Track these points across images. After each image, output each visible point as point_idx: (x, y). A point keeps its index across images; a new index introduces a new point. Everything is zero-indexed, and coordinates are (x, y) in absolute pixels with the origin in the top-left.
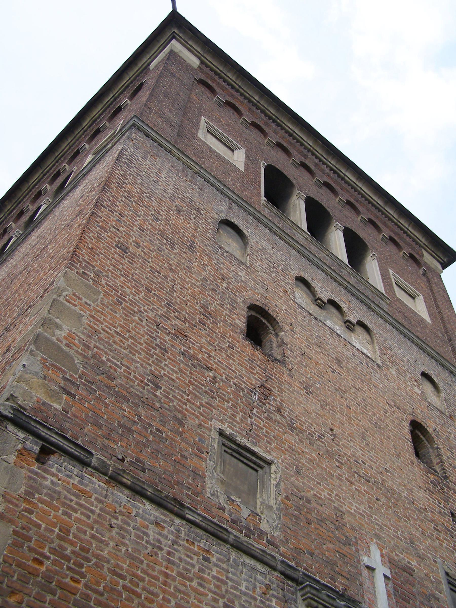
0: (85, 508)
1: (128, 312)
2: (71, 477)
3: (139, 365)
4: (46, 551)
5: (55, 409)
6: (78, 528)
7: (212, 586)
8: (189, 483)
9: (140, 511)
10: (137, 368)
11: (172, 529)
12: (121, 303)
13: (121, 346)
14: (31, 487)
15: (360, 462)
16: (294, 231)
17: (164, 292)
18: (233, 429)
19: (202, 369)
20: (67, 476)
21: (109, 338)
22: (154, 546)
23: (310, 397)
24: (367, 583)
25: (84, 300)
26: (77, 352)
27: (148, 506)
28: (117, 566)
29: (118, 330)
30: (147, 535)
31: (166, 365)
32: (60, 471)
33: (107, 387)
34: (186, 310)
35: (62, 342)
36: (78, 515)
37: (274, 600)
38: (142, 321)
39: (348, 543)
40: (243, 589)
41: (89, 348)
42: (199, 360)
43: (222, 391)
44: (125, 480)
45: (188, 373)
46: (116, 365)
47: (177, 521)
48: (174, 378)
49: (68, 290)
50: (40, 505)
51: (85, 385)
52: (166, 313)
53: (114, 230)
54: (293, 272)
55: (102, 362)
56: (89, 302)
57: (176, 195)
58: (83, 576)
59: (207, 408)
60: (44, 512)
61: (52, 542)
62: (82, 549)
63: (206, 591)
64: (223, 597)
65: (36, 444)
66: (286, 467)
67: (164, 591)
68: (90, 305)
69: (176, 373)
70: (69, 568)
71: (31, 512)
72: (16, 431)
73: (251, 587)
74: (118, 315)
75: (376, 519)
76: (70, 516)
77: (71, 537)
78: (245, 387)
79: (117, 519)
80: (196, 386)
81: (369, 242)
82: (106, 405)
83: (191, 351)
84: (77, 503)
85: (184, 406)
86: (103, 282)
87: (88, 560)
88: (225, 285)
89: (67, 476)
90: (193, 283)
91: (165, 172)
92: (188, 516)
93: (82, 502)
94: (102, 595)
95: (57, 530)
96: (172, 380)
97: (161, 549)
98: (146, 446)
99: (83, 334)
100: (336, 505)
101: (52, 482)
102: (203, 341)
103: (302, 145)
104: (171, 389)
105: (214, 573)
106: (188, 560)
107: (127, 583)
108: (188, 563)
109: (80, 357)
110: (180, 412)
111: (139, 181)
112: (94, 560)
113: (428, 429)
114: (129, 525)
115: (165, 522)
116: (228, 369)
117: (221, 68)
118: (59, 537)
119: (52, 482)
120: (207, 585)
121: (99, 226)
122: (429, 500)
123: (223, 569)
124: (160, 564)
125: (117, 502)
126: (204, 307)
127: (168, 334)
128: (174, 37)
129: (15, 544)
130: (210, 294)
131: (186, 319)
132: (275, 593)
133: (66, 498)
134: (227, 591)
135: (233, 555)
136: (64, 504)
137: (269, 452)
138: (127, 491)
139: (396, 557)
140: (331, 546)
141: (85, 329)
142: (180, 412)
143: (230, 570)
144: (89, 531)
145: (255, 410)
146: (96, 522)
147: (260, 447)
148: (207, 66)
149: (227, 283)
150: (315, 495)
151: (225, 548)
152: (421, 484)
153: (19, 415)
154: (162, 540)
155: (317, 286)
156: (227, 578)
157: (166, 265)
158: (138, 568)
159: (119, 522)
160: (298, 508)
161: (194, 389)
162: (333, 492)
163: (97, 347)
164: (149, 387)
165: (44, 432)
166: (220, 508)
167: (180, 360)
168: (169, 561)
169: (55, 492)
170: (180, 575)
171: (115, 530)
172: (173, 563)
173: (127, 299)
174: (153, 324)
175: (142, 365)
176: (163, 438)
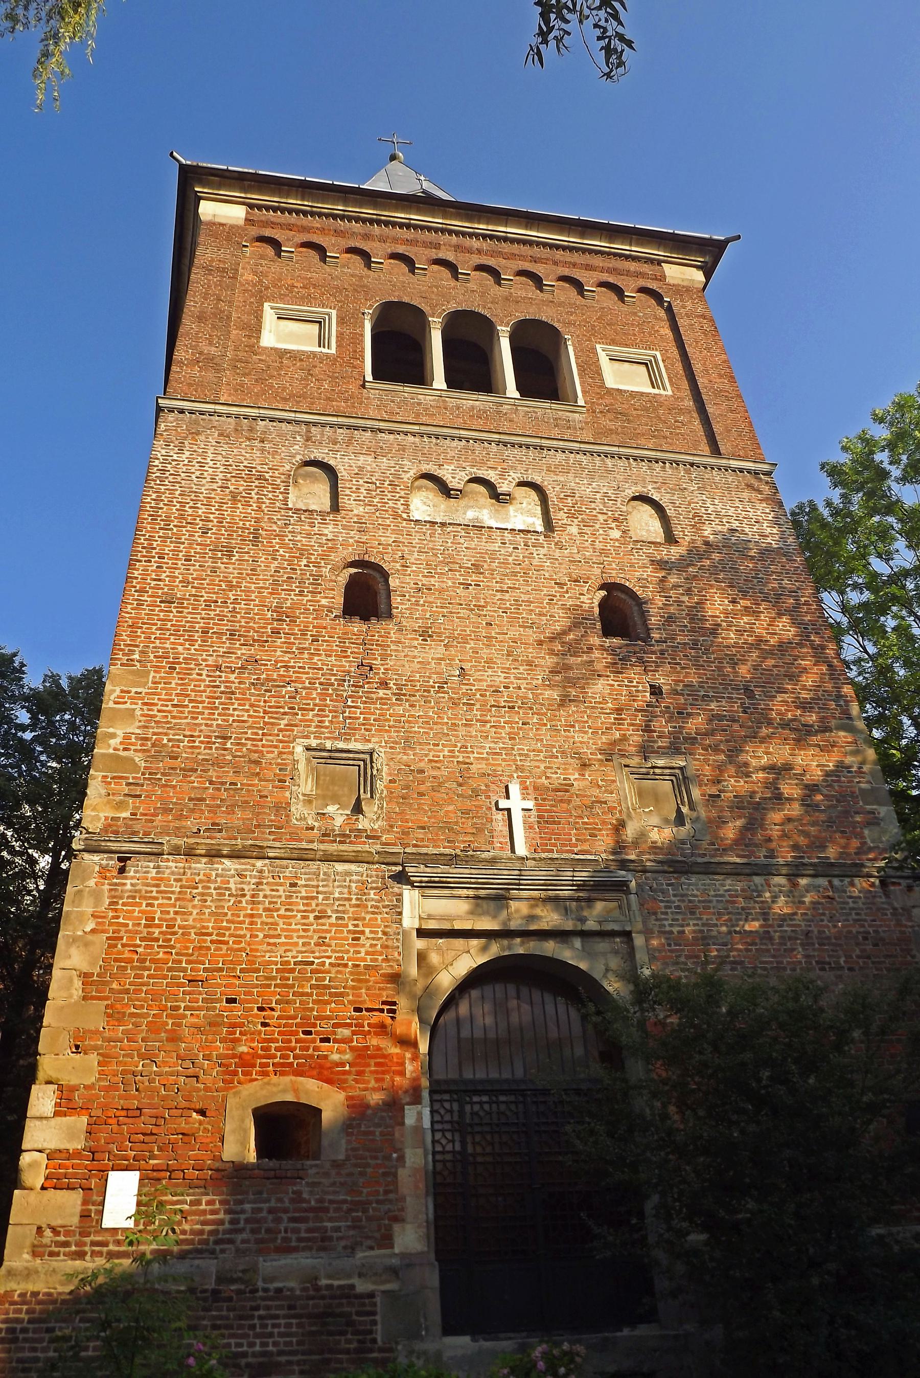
0: (166, 892)
1: (185, 674)
2: (147, 872)
3: (203, 727)
4: (138, 942)
5: (124, 818)
6: (161, 912)
7: (302, 908)
8: (272, 821)
9: (220, 871)
10: (201, 731)
11: (254, 873)
12: (175, 668)
13: (180, 718)
14: (114, 897)
15: (502, 689)
16: (420, 397)
17: (225, 622)
18: (320, 738)
19: (278, 689)
20: (145, 872)
21: (166, 717)
22: (237, 896)
23: (428, 643)
24: (500, 825)
25: (134, 690)
26: (135, 751)
27: (226, 862)
28: (204, 927)
29: (175, 702)
30: (229, 889)
31: (234, 710)
32: (136, 872)
33: (172, 768)
34: (253, 628)
35: (118, 750)
36: (160, 901)
37: (372, 892)
38: (201, 675)
39: (476, 793)
40: (337, 895)
41: (147, 739)
42: (275, 680)
43: (304, 702)
44: (198, 852)
45: (262, 704)
46: (179, 740)
47: (259, 864)
48: (245, 718)
49: (115, 691)
50: (125, 908)
51: (149, 779)
52: (230, 648)
53: (155, 582)
54: (408, 475)
55: (164, 745)
56: (139, 690)
57: (229, 475)
58: (173, 947)
59: (287, 730)
60: (128, 911)
61: (141, 932)
62: (168, 927)
63: (295, 913)
64: (313, 911)
65: (111, 859)
66: (391, 748)
67: (251, 930)
68: (140, 693)
69: (248, 711)
70: (159, 947)
71: (118, 917)
72: (91, 857)
73: (346, 890)
74: (173, 685)
75: (519, 749)
76: (152, 905)
77: (157, 922)
78: (336, 680)
79: (197, 888)
80: (271, 713)
81: (559, 321)
82: (174, 787)
83: (264, 676)
84: (158, 892)
85: (260, 743)
86: (152, 656)
87: (174, 933)
88: (304, 562)
89: (145, 872)
90: (262, 588)
91: (211, 450)
92: (270, 855)
93: (163, 888)
94: (192, 955)
95: (143, 922)
96: (244, 721)
97: (244, 895)
98: (219, 806)
99: (139, 727)
100: (461, 759)
101: (132, 885)
102: (279, 653)
104: (242, 733)
105: (304, 894)
106: (274, 893)
107: (214, 937)
108: (273, 897)
109: (140, 754)
110: (255, 752)
111: (178, 493)
112: (181, 931)
113: (627, 584)
114: (209, 888)
115: (246, 870)
116: (311, 671)
118: (146, 926)
119: (132, 885)
120: (295, 908)
121: (136, 591)
122: (613, 685)
123: (313, 886)
124: (246, 909)
125: (195, 874)
126: (278, 610)
127: (233, 672)
128: (201, 198)
129: (110, 946)
130: (285, 587)
131: (254, 641)
132: (374, 885)
133: (147, 892)
134: (317, 905)
135: (324, 867)
136: (145, 898)
137: (369, 741)
138: (204, 860)
139: (546, 782)
140: (451, 808)
141: (140, 721)
142: (255, 752)
143: (321, 884)
144: (172, 910)
145: (350, 700)
146: (177, 899)
147: (356, 740)
148: (260, 207)
149: (308, 558)
150: (430, 761)
151: (314, 866)
153: (90, 842)
154: (245, 886)
155: (446, 473)
156: (318, 893)
157: (224, 587)
158: (222, 921)
159: (200, 890)
160: (407, 787)
161: (270, 718)
162: (456, 746)
163: (154, 734)
164: (217, 745)
165: (114, 846)
166: (308, 829)
167: (252, 695)
168: (253, 903)
169: (136, 891)
170: (265, 910)
171: (198, 898)
172: (259, 903)
173: (181, 660)
174: (214, 671)
175: (206, 725)
176: (238, 789)
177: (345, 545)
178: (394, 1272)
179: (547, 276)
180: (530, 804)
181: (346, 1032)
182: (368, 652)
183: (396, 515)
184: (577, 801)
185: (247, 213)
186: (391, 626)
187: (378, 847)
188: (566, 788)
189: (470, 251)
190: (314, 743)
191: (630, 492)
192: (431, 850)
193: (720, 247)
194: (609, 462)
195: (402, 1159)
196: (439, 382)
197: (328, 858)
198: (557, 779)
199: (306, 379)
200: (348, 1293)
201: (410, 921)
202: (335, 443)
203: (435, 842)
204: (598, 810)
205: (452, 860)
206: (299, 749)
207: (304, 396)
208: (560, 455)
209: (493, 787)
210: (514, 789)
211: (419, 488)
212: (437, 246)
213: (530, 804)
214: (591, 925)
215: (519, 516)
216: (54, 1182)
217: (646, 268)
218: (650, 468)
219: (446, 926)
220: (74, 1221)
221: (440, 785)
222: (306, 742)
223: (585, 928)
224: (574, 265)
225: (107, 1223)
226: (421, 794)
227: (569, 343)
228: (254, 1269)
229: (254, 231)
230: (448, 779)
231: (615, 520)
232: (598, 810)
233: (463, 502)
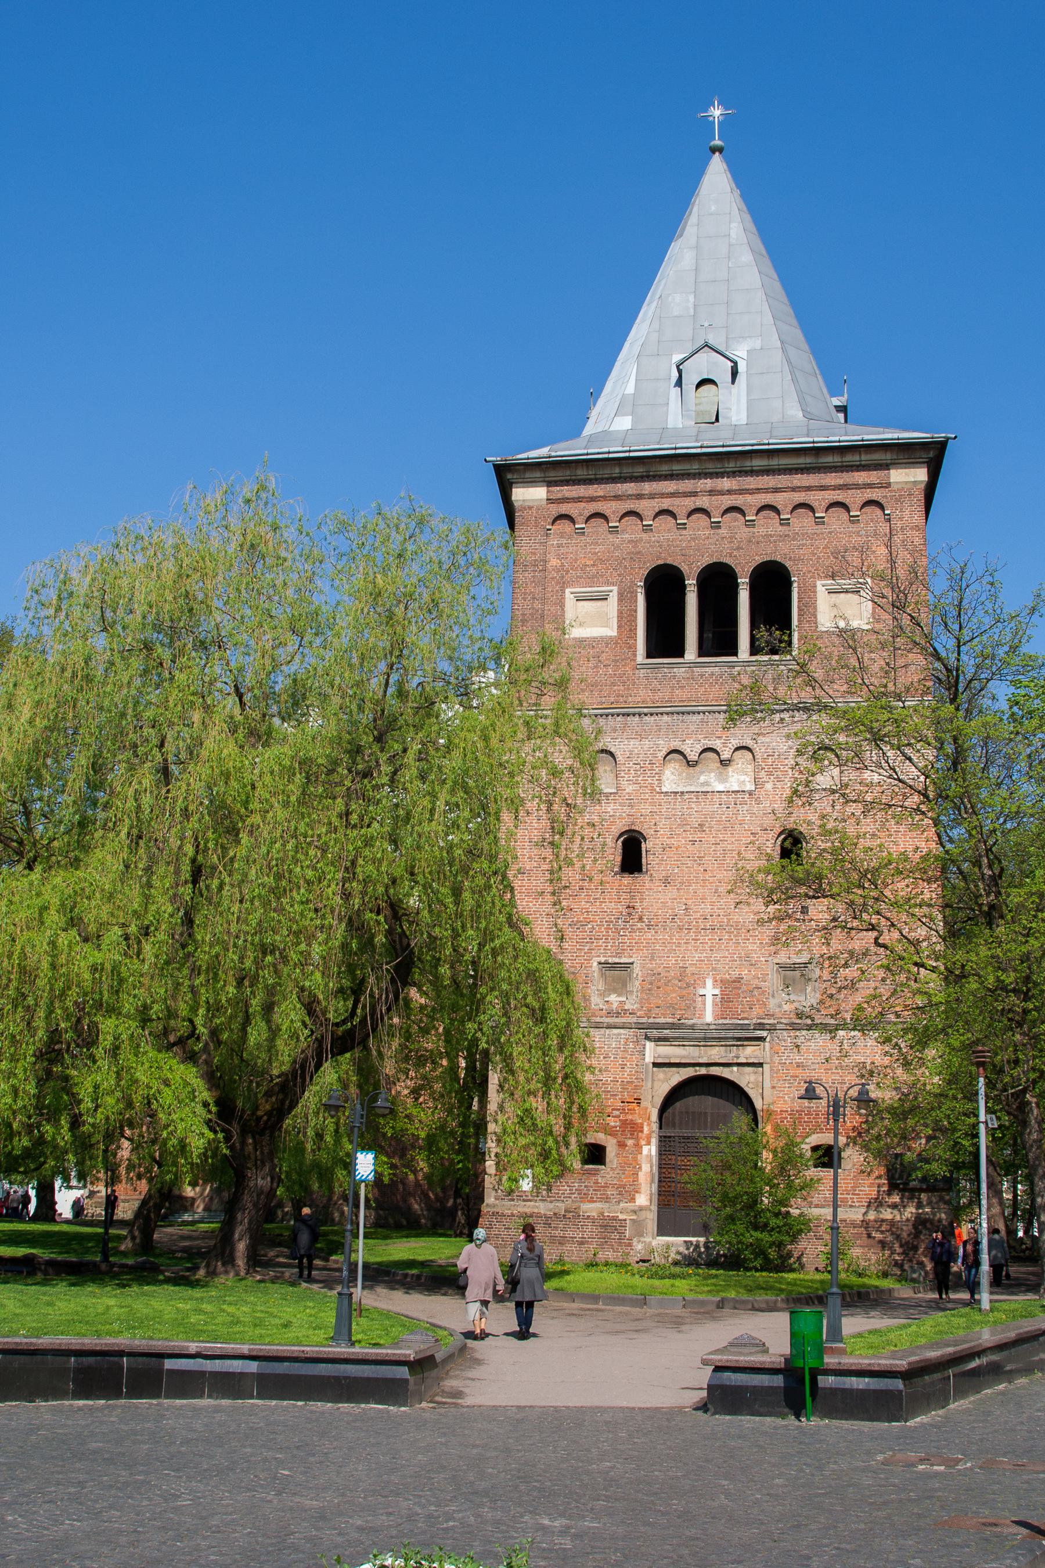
24: (699, 1005)
39: (688, 985)
117: (568, 473)
128: (512, 483)
135: (608, 1031)
140: (674, 995)
160: (651, 984)
177: (621, 818)
178: (635, 1212)
180: (717, 992)
181: (618, 1113)
182: (632, 897)
183: (653, 790)
184: (744, 988)
186: (647, 877)
187: (635, 1020)
188: (738, 980)
189: (721, 493)
190: (603, 960)
192: (662, 1020)
193: (941, 447)
195: (640, 1168)
196: (691, 652)
197: (610, 1027)
198: (735, 974)
199: (595, 667)
200: (615, 1218)
201: (649, 1059)
202: (615, 730)
203: (665, 1016)
204: (756, 993)
205: (672, 1026)
206: (595, 964)
207: (596, 684)
209: (698, 982)
210: (709, 982)
211: (670, 761)
212: (694, 494)
213: (717, 992)
214: (742, 1060)
215: (735, 775)
217: (873, 477)
219: (667, 1061)
221: (669, 981)
222: (598, 959)
223: (740, 1061)
224: (809, 489)
226: (659, 988)
227: (795, 585)
228: (579, 1207)
229: (556, 510)
230: (674, 978)
232: (756, 993)
233: (697, 768)
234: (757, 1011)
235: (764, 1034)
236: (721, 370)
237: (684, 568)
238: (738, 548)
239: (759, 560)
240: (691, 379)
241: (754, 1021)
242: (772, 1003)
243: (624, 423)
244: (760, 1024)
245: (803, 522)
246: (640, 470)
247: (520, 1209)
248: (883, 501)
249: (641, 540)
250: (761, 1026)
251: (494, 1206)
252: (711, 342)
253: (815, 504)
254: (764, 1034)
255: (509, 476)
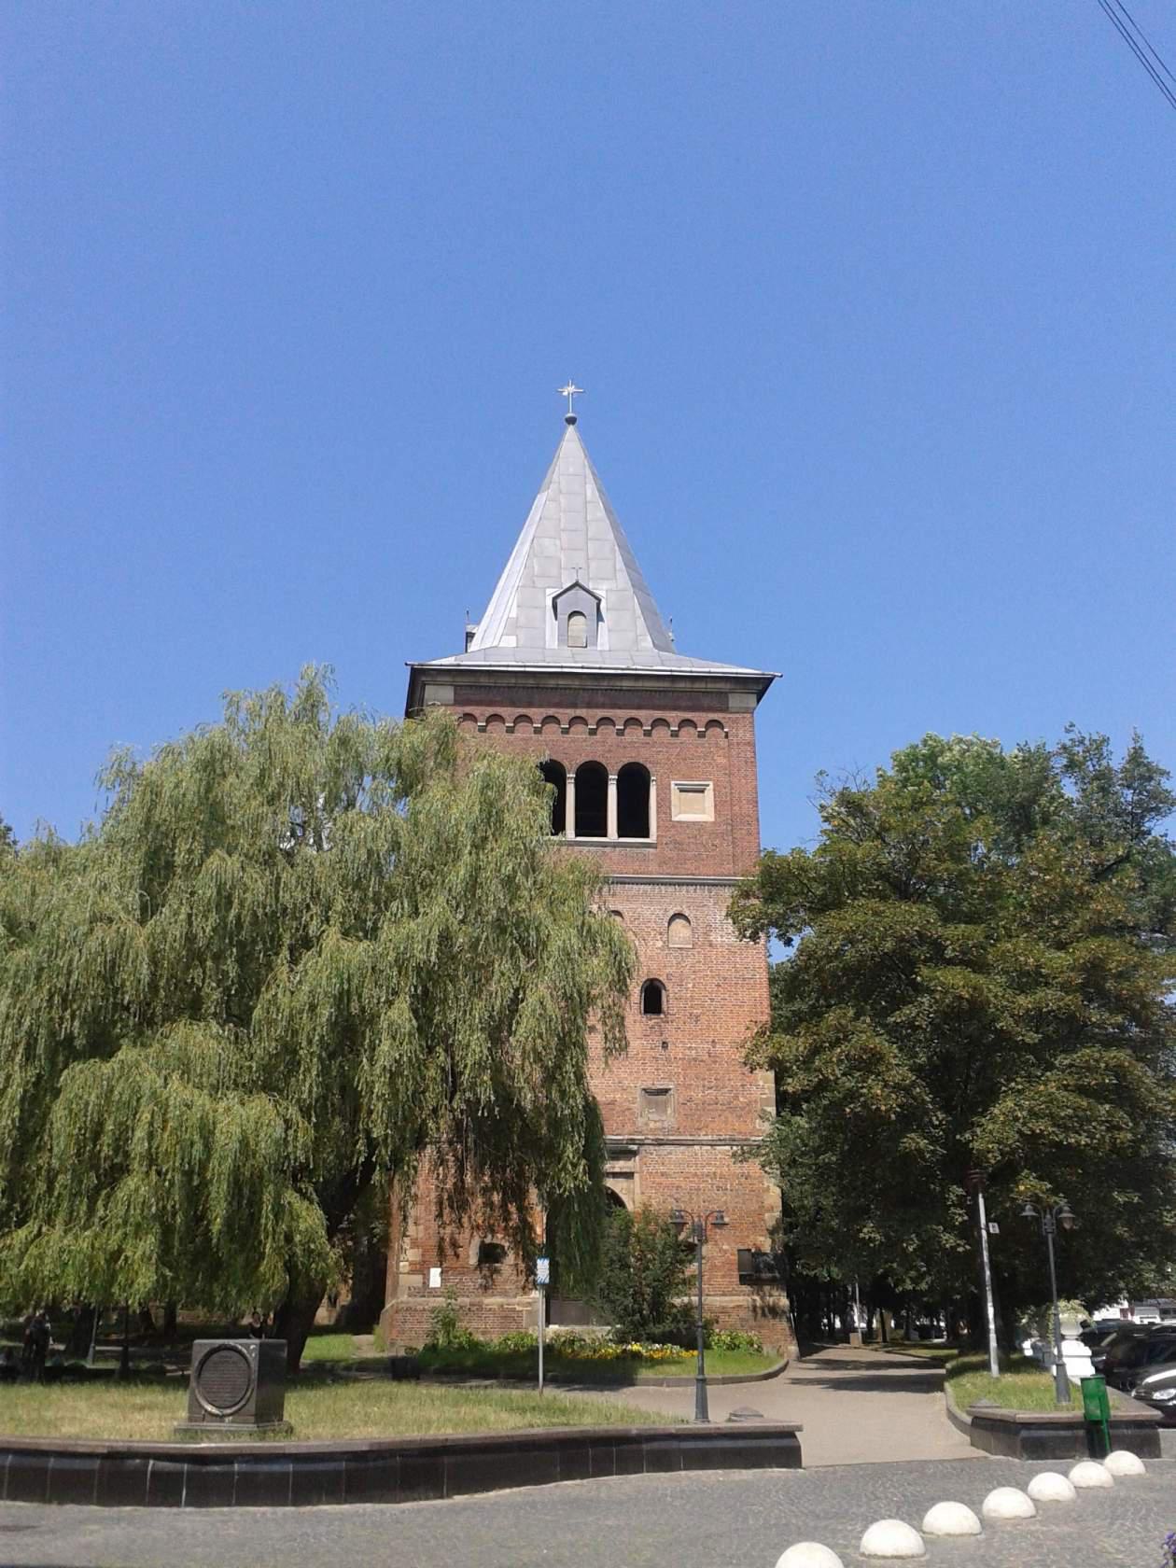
103: (570, 689)
152: (639, 1035)
178: (530, 1304)
179: (647, 720)
185: (455, 694)
191: (671, 913)
194: (663, 887)
200: (514, 1310)
204: (627, 1113)
208: (635, 886)
214: (617, 1170)
216: (412, 1272)
218: (687, 891)
220: (420, 1285)
225: (432, 1285)
231: (661, 934)
232: (627, 1113)
234: (628, 1128)
235: (635, 1147)
236: (587, 605)
237: (566, 763)
238: (610, 751)
239: (626, 761)
240: (564, 609)
241: (626, 1137)
242: (640, 1121)
243: (510, 642)
244: (632, 1140)
245: (661, 734)
246: (531, 682)
247: (431, 1305)
248: (722, 721)
249: (531, 738)
250: (633, 1142)
251: (408, 1303)
252: (581, 582)
253: (670, 720)
254: (635, 1147)
255: (424, 679)
